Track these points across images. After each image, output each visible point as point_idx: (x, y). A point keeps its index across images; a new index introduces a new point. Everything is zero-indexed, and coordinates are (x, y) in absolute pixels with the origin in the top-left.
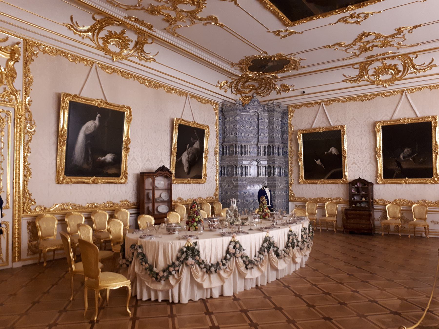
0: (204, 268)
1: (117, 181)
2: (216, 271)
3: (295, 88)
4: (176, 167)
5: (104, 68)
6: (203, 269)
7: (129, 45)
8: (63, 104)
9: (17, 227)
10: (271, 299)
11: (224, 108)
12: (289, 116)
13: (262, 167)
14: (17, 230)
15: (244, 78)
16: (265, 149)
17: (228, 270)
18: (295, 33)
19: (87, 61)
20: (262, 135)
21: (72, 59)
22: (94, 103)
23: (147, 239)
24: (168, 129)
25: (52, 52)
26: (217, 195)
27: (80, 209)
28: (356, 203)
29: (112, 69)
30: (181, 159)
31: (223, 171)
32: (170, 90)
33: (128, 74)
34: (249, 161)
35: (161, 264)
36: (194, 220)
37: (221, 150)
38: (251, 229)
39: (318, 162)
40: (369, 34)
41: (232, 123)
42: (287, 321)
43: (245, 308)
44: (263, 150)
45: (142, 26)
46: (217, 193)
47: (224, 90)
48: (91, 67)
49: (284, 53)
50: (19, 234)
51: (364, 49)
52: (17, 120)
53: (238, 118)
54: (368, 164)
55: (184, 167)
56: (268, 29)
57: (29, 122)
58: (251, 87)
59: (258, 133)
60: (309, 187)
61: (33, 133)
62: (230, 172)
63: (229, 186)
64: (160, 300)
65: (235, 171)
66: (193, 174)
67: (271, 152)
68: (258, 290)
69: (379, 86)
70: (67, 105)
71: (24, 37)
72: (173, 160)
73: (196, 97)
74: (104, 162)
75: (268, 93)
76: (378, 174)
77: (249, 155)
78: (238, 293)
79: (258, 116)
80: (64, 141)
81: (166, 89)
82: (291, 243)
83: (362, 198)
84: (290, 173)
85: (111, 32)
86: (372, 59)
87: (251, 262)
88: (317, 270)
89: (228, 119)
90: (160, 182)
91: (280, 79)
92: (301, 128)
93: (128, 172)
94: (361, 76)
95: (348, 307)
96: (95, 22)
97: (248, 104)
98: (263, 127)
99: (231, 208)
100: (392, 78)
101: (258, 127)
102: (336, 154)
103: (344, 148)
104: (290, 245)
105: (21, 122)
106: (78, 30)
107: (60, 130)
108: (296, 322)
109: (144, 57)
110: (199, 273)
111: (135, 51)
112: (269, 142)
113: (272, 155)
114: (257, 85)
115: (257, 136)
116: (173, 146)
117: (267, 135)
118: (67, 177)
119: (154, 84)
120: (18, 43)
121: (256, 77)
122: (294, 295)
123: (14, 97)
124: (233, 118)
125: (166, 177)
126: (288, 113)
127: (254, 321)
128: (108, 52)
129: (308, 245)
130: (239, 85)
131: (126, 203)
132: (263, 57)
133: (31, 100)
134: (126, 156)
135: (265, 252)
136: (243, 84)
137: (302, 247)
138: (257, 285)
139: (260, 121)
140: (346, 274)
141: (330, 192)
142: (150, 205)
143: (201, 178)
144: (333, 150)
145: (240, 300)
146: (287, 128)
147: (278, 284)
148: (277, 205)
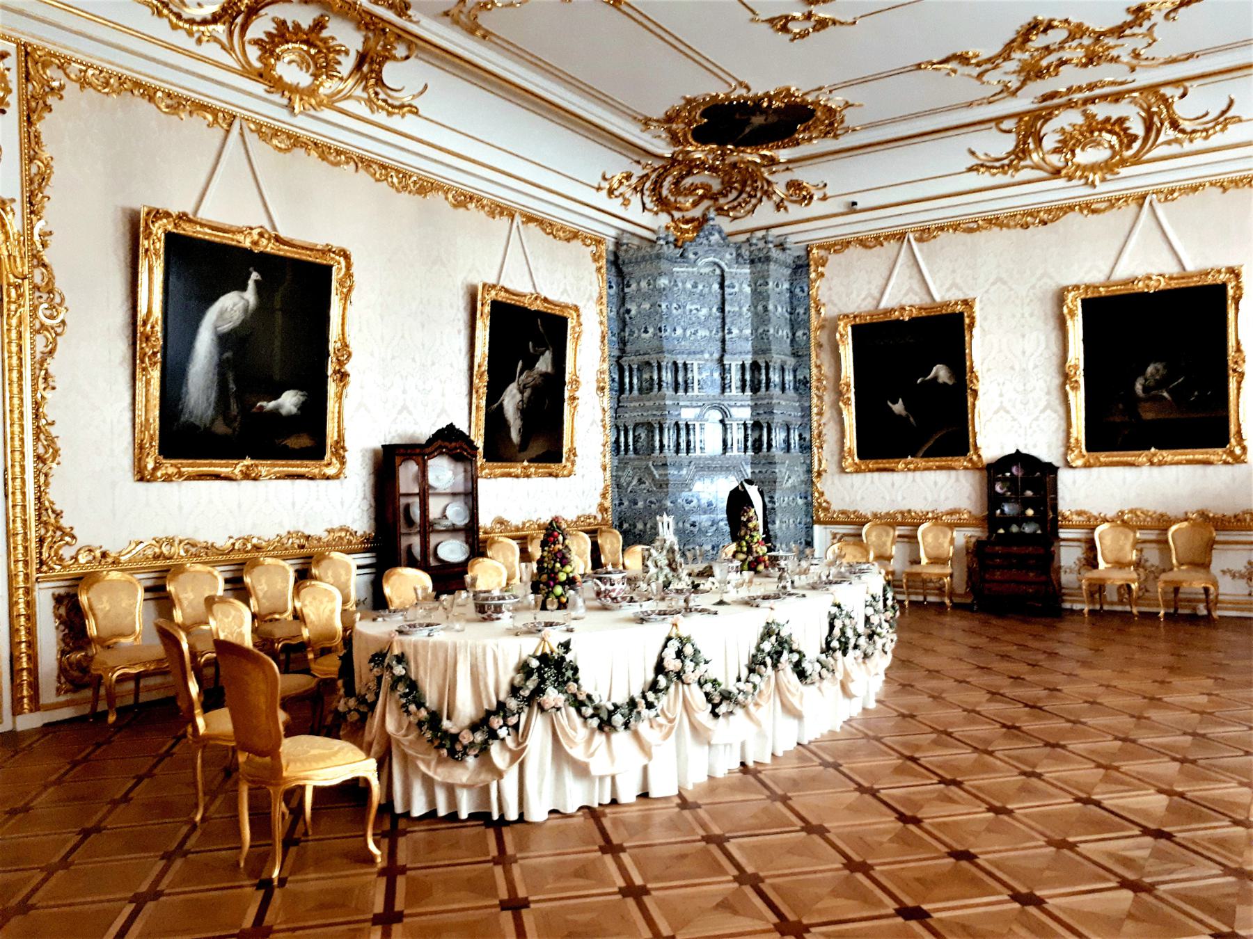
0: (592, 716)
1: (316, 471)
2: (626, 725)
5: (267, 133)
6: (590, 721)
7: (339, 63)
8: (146, 243)
9: (23, 611)
10: (790, 802)
11: (622, 254)
12: (813, 275)
14: (22, 619)
15: (680, 163)
16: (743, 374)
17: (661, 720)
18: (834, 23)
19: (214, 112)
20: (735, 331)
21: (168, 107)
22: (240, 237)
23: (420, 636)
24: (462, 317)
25: (107, 84)
26: (606, 510)
28: (1006, 521)
29: (289, 136)
30: (501, 405)
31: (622, 439)
32: (464, 199)
33: (339, 152)
34: (698, 410)
35: (466, 708)
36: (553, 575)
37: (616, 377)
38: (721, 603)
39: (898, 408)
40: (1050, 26)
41: (646, 297)
42: (846, 866)
43: (716, 830)
44: (739, 376)
46: (608, 504)
47: (620, 200)
48: (228, 131)
49: (800, 86)
50: (31, 631)
51: (1032, 72)
52: (8, 290)
54: (1043, 411)
55: (509, 428)
57: (45, 296)
58: (700, 192)
60: (872, 482)
61: (59, 330)
63: (640, 481)
64: (464, 815)
65: (657, 438)
67: (760, 382)
68: (750, 778)
69: (1074, 182)
70: (160, 246)
71: (17, 35)
72: (477, 407)
74: (275, 413)
75: (749, 207)
76: (1072, 440)
78: (690, 787)
80: (155, 354)
81: (450, 196)
82: (837, 644)
84: (816, 443)
85: (284, 23)
86: (1056, 101)
87: (726, 696)
88: (913, 717)
89: (634, 286)
90: (443, 473)
91: (784, 167)
92: (847, 311)
93: (346, 445)
94: (1021, 152)
95: (1018, 820)
97: (693, 240)
98: (737, 309)
99: (657, 544)
100: (1112, 157)
101: (722, 310)
102: (950, 382)
105: (20, 296)
106: (185, 16)
107: (140, 322)
108: (871, 867)
109: (385, 101)
110: (576, 731)
112: (755, 353)
113: (763, 389)
114: (716, 185)
115: (720, 334)
116: (476, 368)
117: (748, 332)
118: (168, 462)
119: (415, 183)
121: (715, 159)
122: (856, 790)
125: (456, 458)
126: (808, 265)
127: (750, 869)
128: (277, 85)
130: (666, 184)
131: (343, 534)
132: (738, 99)
133: (47, 229)
134: (339, 397)
135: (766, 666)
136: (677, 183)
137: (869, 651)
138: (743, 764)
139: (727, 290)
140: (998, 726)
142: (416, 541)
144: (941, 372)
145: (699, 807)
146: (807, 310)
147: (802, 758)
148: (779, 534)
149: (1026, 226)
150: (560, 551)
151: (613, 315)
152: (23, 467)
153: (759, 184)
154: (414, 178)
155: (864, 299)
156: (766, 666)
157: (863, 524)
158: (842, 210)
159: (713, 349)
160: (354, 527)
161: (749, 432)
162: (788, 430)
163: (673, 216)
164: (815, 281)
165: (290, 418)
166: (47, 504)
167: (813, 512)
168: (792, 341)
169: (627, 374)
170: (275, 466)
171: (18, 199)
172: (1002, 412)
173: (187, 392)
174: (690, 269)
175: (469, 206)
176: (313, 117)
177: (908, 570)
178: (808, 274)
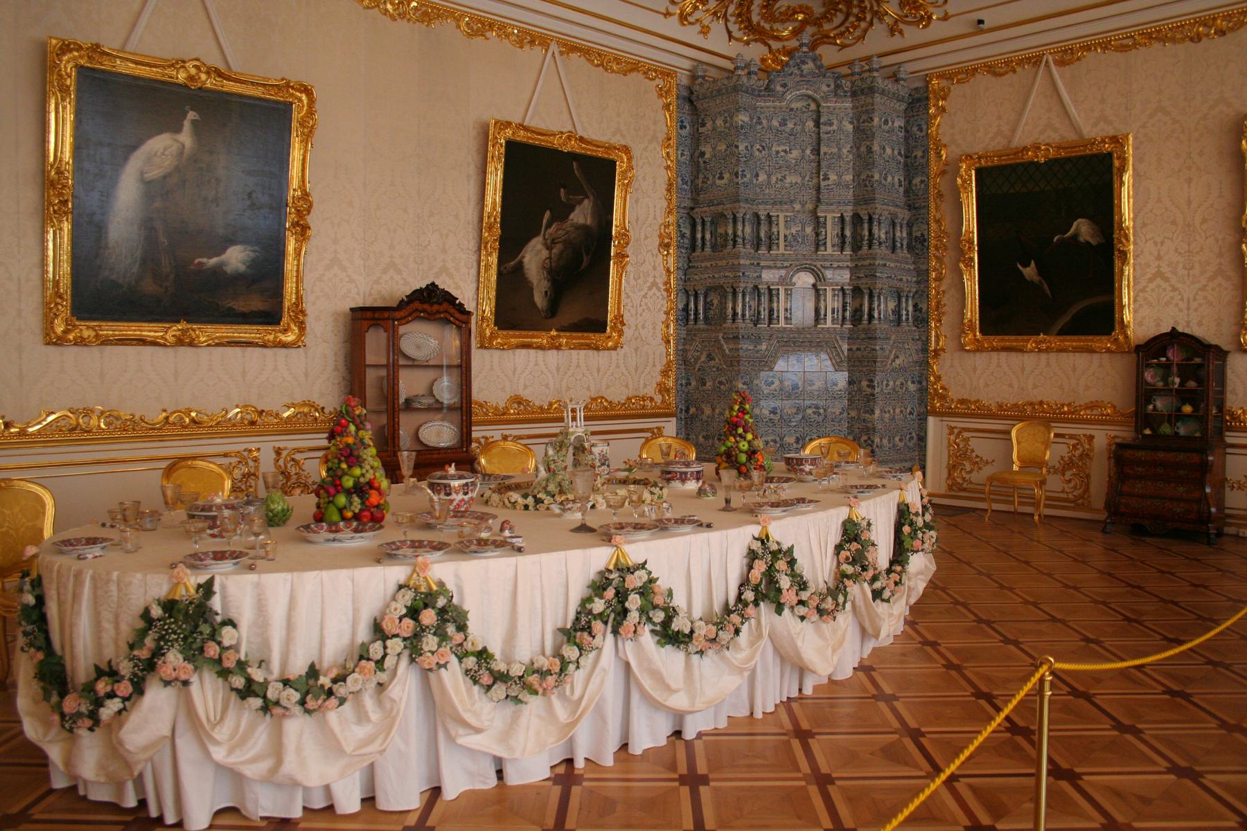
1: (271, 337)
3: (951, 8)
4: (498, 291)
11: (696, 88)
13: (829, 294)
16: (843, 229)
20: (833, 177)
26: (668, 391)
31: (692, 305)
34: (783, 272)
37: (688, 232)
39: (1030, 272)
44: (837, 230)
46: (671, 383)
47: (697, 27)
53: (742, 118)
54: (1211, 279)
58: (800, 17)
59: (818, 173)
63: (710, 357)
65: (730, 305)
66: (572, 311)
73: (586, 52)
74: (218, 271)
75: (858, 33)
77: (782, 250)
80: (65, 202)
83: (1184, 404)
89: (709, 125)
92: (969, 151)
98: (835, 150)
101: (817, 151)
102: (1093, 242)
103: (1121, 222)
112: (857, 202)
115: (815, 181)
116: (486, 219)
117: (849, 177)
118: (82, 325)
119: (416, 8)
124: (725, 122)
126: (927, 99)
131: (306, 410)
139: (823, 128)
141: (1073, 377)
143: (605, 331)
144: (1083, 228)
146: (926, 152)
148: (879, 426)
150: (348, 445)
155: (993, 139)
156: (606, 623)
158: (971, 30)
161: (848, 300)
163: (770, 47)
164: (935, 117)
165: (238, 278)
168: (907, 192)
174: (777, 104)
175: (488, 34)
178: (927, 109)
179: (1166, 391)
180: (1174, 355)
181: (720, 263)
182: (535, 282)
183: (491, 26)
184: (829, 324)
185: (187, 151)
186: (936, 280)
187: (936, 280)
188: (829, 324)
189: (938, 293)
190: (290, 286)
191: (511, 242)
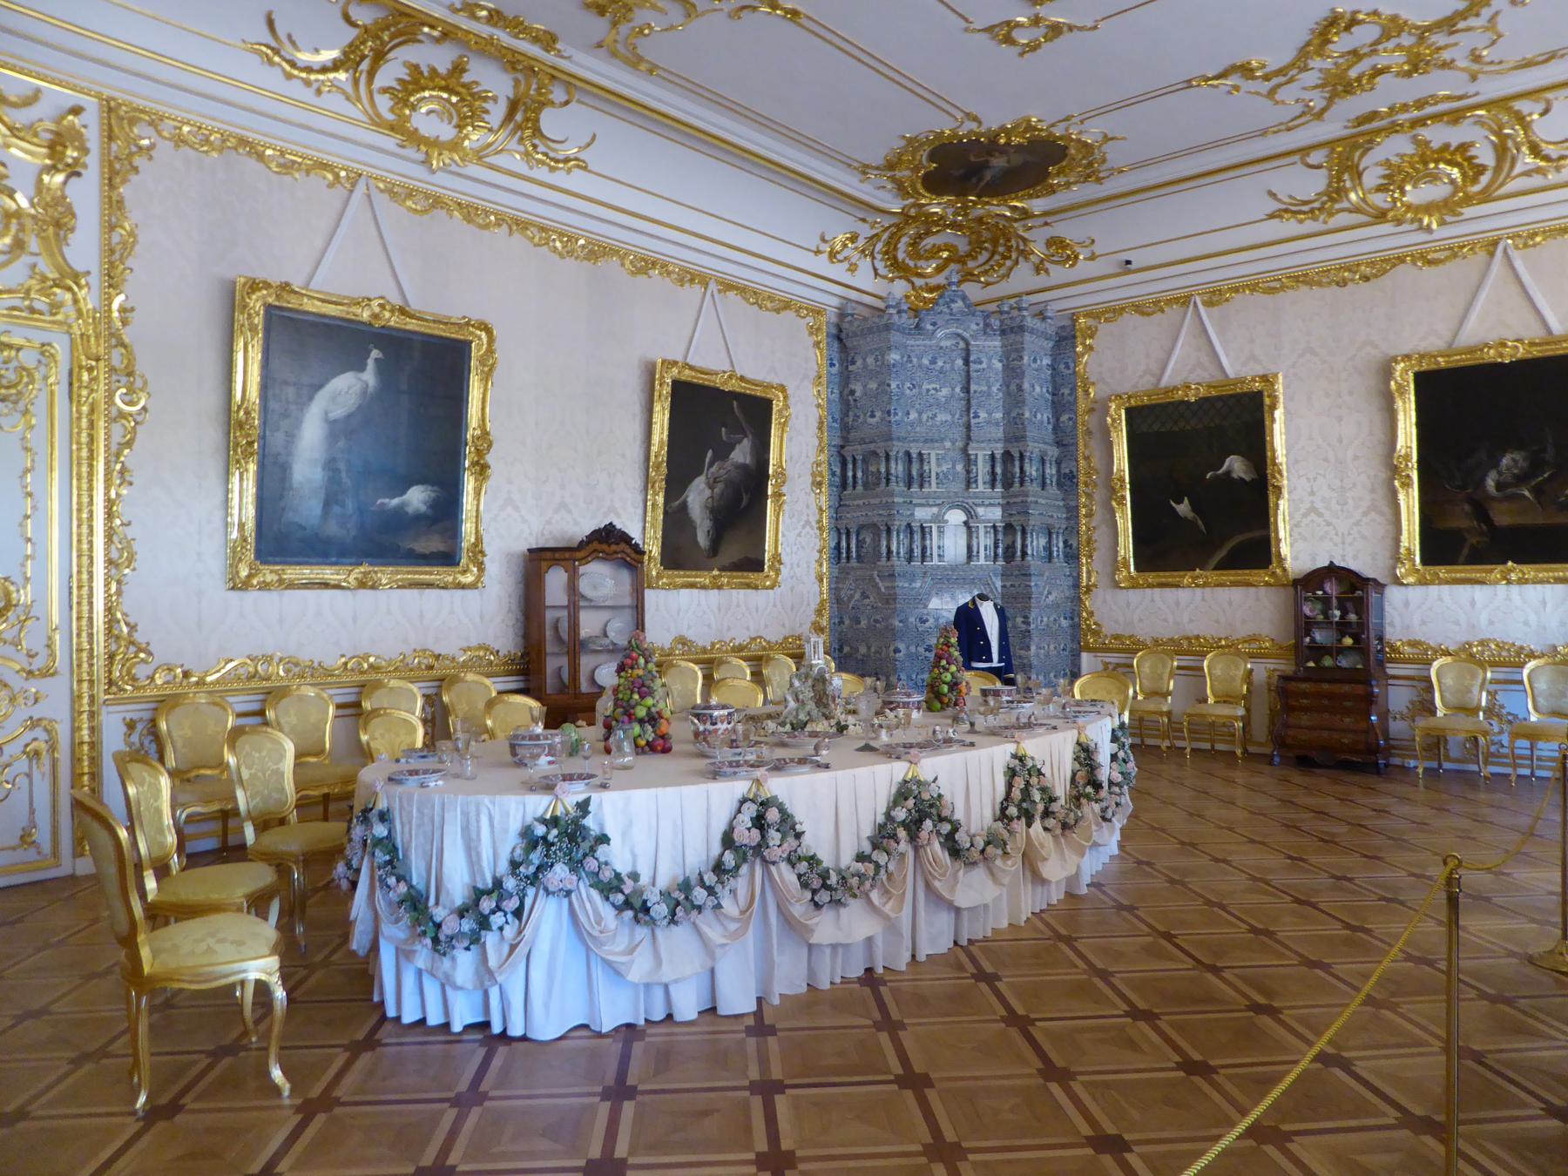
3: (1097, 249)
4: (664, 530)
7: (487, 112)
9: (86, 739)
11: (845, 326)
12: (1080, 349)
14: (86, 748)
16: (993, 467)
18: (1071, 28)
20: (983, 415)
21: (279, 165)
25: (207, 141)
27: (318, 674)
28: (1318, 651)
29: (427, 196)
30: (685, 504)
31: (844, 544)
32: (645, 265)
33: (487, 213)
34: (935, 510)
37: (838, 470)
39: (1184, 508)
41: (873, 374)
44: (988, 468)
45: (516, 37)
46: (824, 622)
47: (846, 265)
49: (1042, 115)
51: (1339, 86)
52: (79, 374)
53: (894, 356)
56: (966, 20)
57: (124, 380)
58: (945, 254)
59: (968, 410)
61: (139, 419)
62: (864, 543)
63: (864, 596)
66: (732, 552)
69: (1405, 227)
70: (258, 320)
71: (98, 88)
73: (742, 290)
75: (1003, 271)
79: (967, 351)
80: (250, 444)
84: (1084, 551)
85: (417, 67)
86: (1376, 124)
89: (859, 363)
92: (1120, 390)
93: (486, 548)
94: (1335, 192)
96: (352, 33)
101: (966, 389)
102: (1247, 478)
103: (1274, 458)
104: (1013, 811)
105: (94, 380)
106: (299, 64)
109: (545, 154)
111: (513, 133)
112: (1007, 440)
113: (1017, 485)
114: (963, 247)
116: (653, 458)
117: (999, 415)
118: (266, 569)
119: (583, 246)
120: (76, 111)
121: (956, 214)
123: (68, 296)
126: (1074, 337)
128: (415, 139)
129: (1104, 810)
133: (128, 306)
136: (914, 244)
138: (869, 970)
139: (973, 367)
144: (1236, 465)
146: (1073, 390)
148: (1035, 662)
149: (1343, 283)
151: (835, 397)
152: (91, 574)
153: (1013, 242)
154: (582, 242)
157: (1136, 651)
159: (957, 436)
160: (496, 646)
161: (1000, 537)
162: (1050, 534)
164: (1083, 355)
165: (418, 518)
166: (119, 615)
167: (1079, 636)
168: (1056, 429)
169: (850, 466)
170: (397, 573)
171: (95, 270)
172: (1313, 516)
173: (291, 488)
176: (459, 175)
177: (1190, 711)
179: (1328, 622)
180: (1331, 588)
181: (873, 501)
182: (698, 521)
183: (654, 264)
184: (982, 561)
185: (370, 390)
186: (1086, 516)
187: (1086, 516)
188: (982, 561)
189: (1088, 529)
190: (467, 528)
191: (676, 484)
